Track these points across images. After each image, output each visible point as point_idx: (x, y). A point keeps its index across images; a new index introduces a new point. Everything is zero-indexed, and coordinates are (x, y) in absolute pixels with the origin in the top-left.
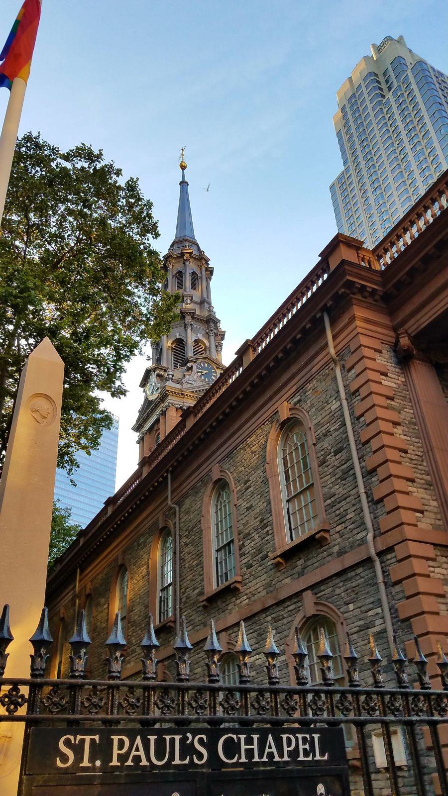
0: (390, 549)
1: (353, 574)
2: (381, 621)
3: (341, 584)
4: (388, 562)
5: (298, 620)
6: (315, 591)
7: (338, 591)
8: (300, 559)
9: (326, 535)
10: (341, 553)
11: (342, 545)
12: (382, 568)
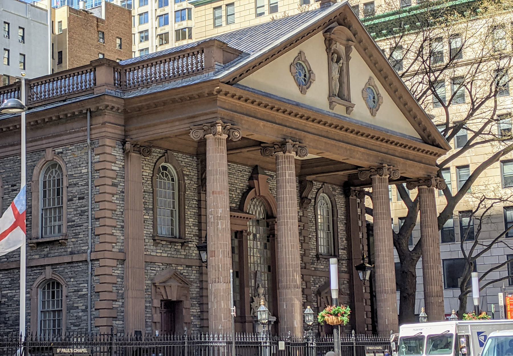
0: (98, 260)
1: (76, 265)
2: (86, 290)
3: (69, 268)
4: (95, 265)
5: (40, 279)
6: (53, 267)
7: (66, 271)
8: (46, 248)
9: (66, 242)
10: (72, 253)
11: (73, 249)
12: (92, 266)
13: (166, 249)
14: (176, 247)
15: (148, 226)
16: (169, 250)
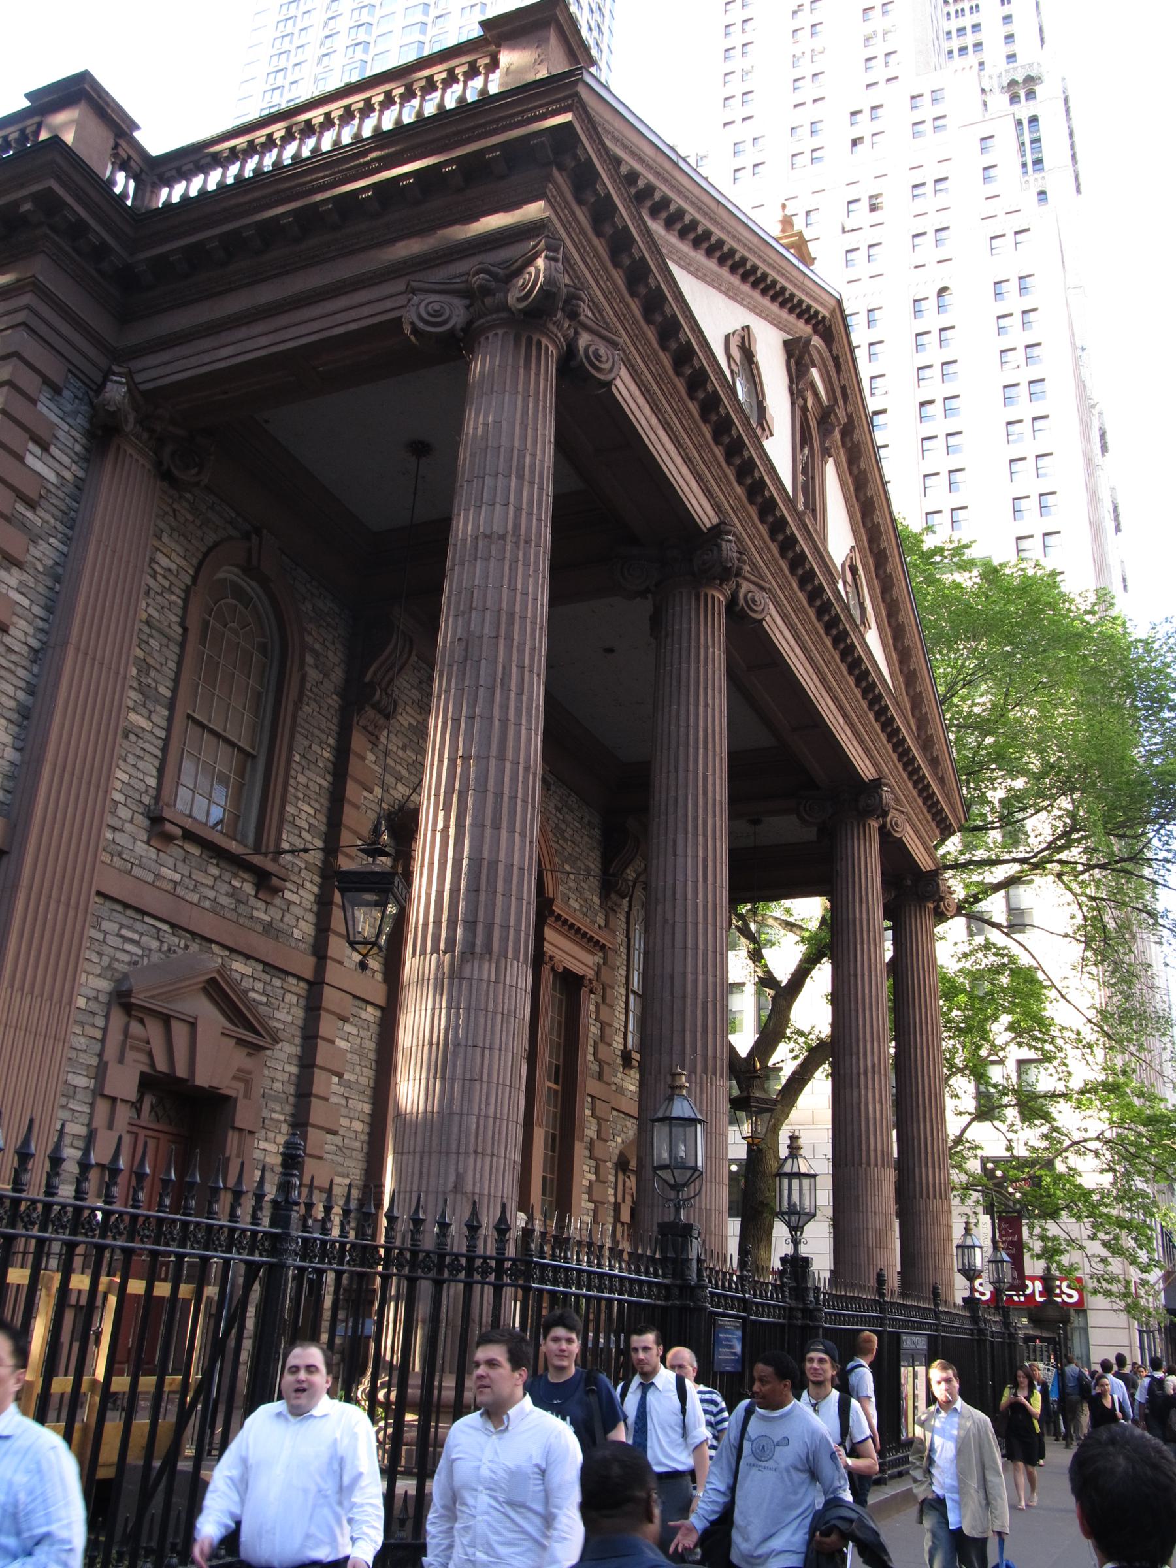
13: (198, 876)
14: (236, 883)
15: (141, 758)
16: (211, 883)
